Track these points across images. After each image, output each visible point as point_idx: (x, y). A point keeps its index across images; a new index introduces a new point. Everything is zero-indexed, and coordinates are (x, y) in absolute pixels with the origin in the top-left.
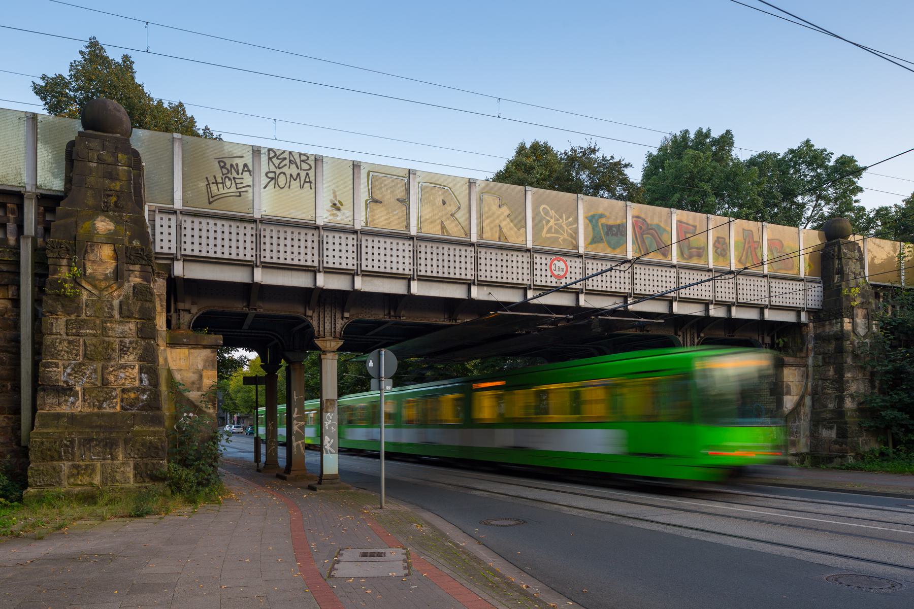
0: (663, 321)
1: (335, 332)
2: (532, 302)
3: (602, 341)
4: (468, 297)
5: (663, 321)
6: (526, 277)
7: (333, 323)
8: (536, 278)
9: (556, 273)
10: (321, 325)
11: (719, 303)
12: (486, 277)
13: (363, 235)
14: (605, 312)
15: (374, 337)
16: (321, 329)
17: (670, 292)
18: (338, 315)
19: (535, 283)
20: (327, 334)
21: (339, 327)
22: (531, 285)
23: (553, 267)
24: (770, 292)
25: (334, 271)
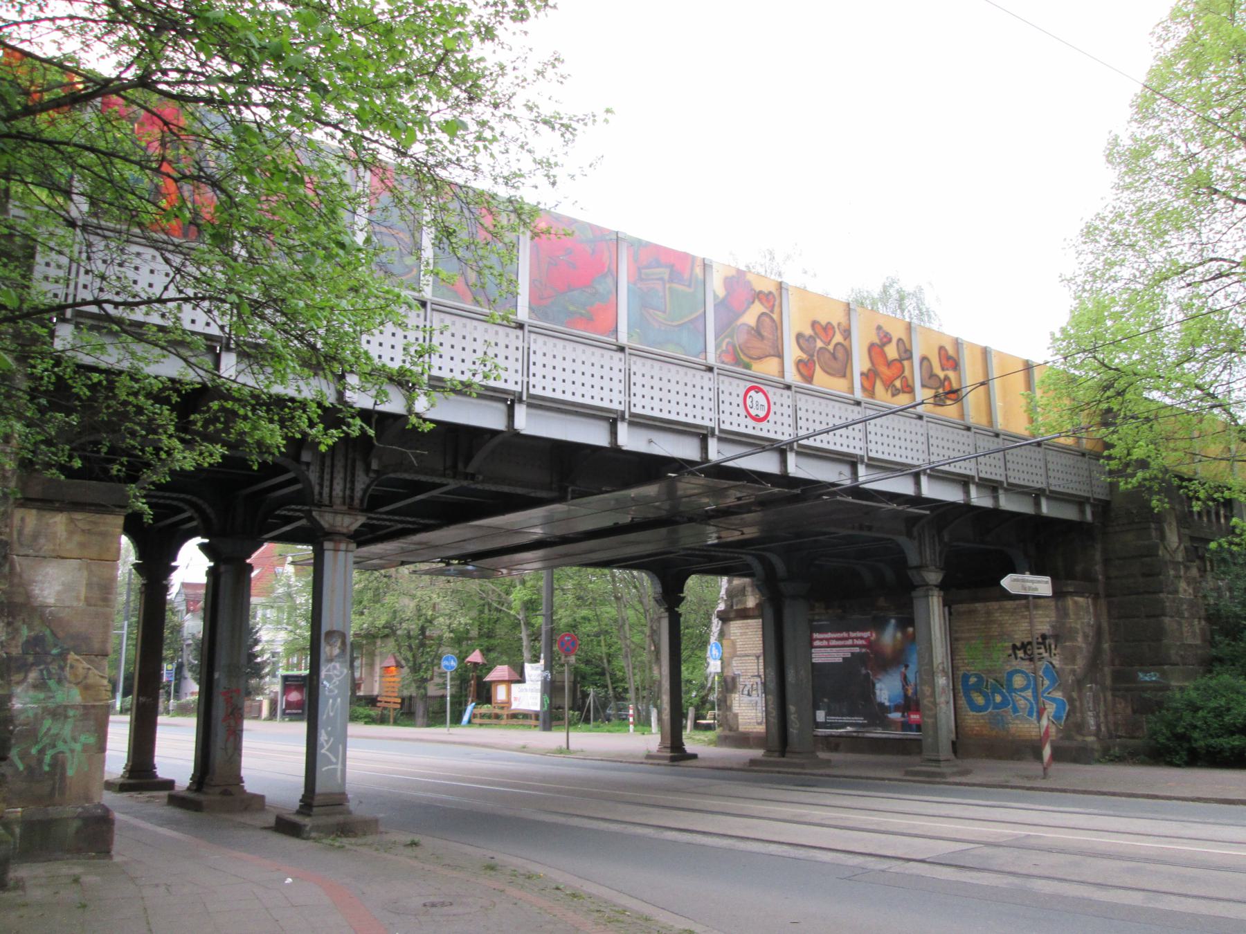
0: (928, 512)
1: (352, 498)
2: (861, 486)
3: (772, 545)
4: (611, 443)
5: (928, 512)
6: (617, 397)
7: (348, 479)
8: (633, 400)
9: (753, 412)
10: (327, 483)
11: (1014, 489)
12: (611, 401)
13: (435, 313)
14: (840, 490)
15: (391, 517)
16: (326, 490)
17: (808, 438)
18: (359, 466)
19: (532, 391)
20: (338, 501)
21: (360, 487)
22: (521, 393)
23: (749, 401)
24: (1047, 470)
25: (883, 465)
